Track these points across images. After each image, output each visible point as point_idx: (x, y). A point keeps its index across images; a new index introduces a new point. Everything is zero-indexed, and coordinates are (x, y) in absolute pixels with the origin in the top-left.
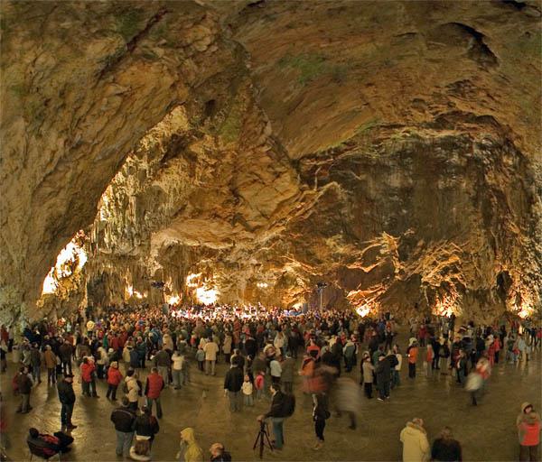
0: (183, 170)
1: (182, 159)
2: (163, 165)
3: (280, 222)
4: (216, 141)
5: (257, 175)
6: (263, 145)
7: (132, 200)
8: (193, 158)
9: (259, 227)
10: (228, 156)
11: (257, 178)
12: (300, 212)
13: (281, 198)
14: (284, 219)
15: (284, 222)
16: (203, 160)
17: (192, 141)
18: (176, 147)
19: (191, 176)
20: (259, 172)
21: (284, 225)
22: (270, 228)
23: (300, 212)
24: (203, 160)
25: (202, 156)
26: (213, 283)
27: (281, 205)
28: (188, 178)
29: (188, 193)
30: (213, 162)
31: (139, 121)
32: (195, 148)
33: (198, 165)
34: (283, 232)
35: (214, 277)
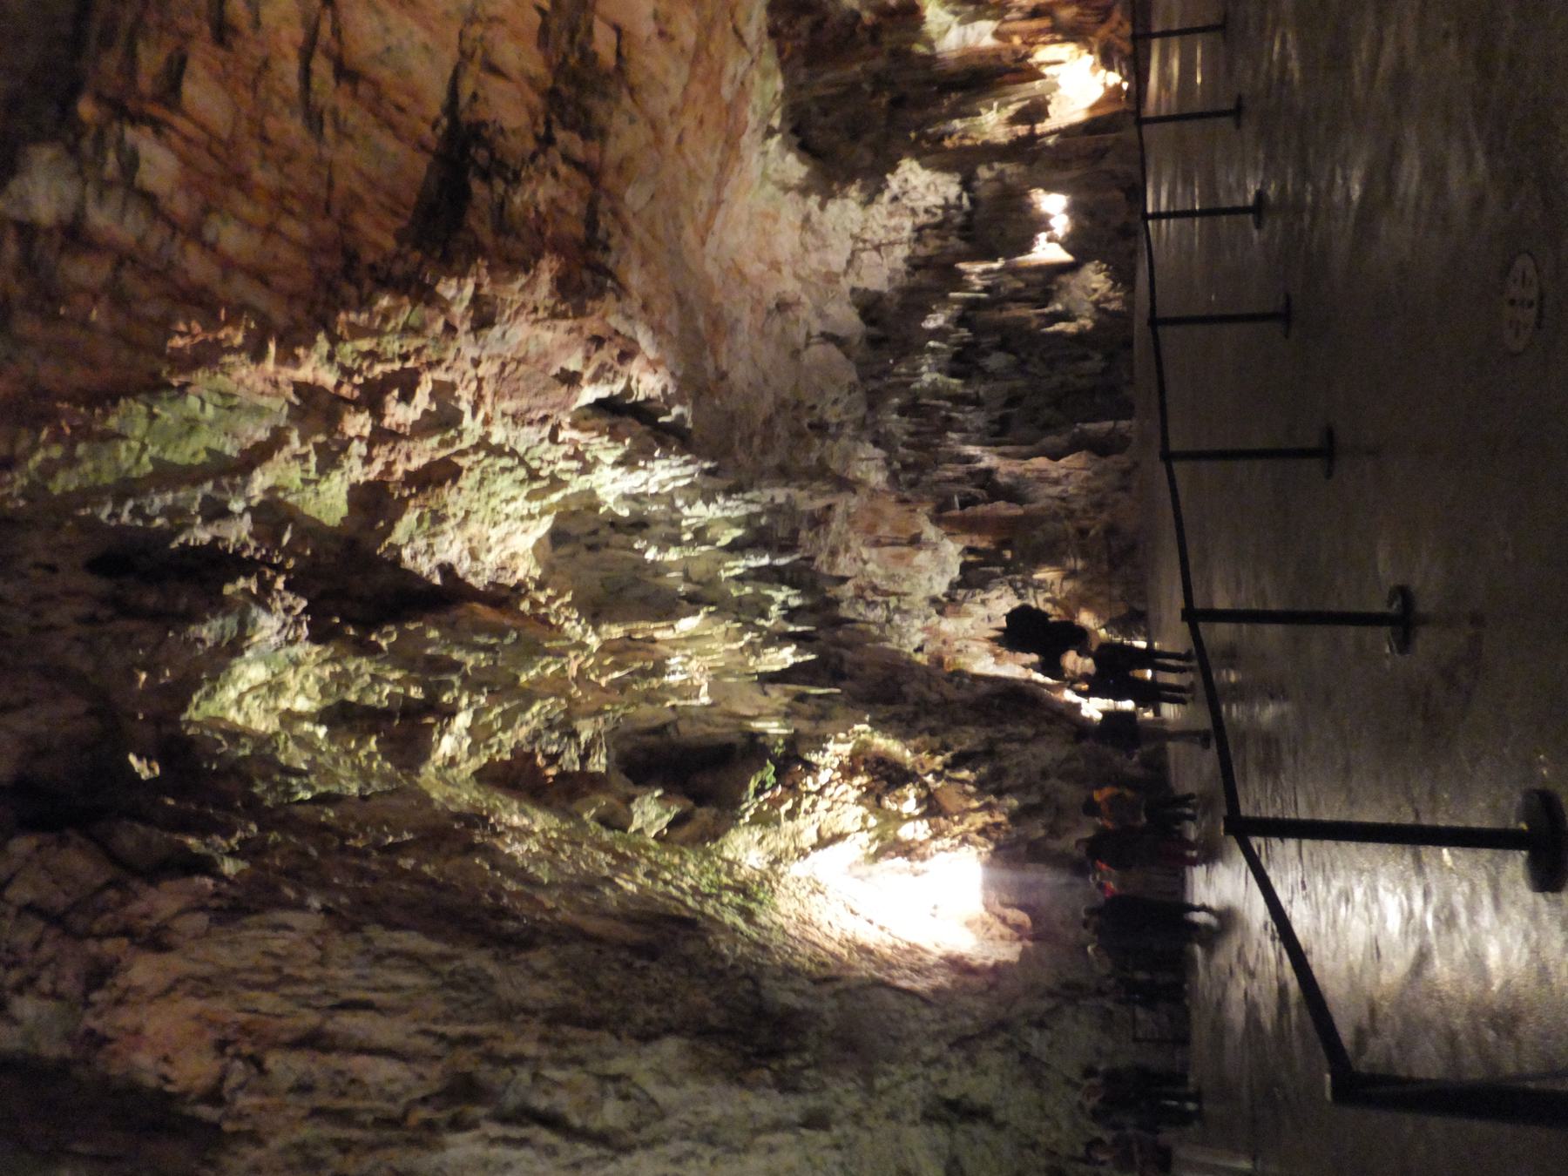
0: (438, 518)
1: (399, 534)
2: (450, 594)
4: (260, 454)
5: (306, 73)
6: (149, 199)
7: (616, 631)
8: (374, 503)
10: (305, 373)
11: (322, 67)
16: (368, 460)
17: (310, 530)
19: (455, 473)
20: (290, 68)
24: (368, 460)
25: (355, 471)
28: (467, 481)
29: (524, 439)
30: (357, 424)
31: (332, 971)
33: (399, 470)
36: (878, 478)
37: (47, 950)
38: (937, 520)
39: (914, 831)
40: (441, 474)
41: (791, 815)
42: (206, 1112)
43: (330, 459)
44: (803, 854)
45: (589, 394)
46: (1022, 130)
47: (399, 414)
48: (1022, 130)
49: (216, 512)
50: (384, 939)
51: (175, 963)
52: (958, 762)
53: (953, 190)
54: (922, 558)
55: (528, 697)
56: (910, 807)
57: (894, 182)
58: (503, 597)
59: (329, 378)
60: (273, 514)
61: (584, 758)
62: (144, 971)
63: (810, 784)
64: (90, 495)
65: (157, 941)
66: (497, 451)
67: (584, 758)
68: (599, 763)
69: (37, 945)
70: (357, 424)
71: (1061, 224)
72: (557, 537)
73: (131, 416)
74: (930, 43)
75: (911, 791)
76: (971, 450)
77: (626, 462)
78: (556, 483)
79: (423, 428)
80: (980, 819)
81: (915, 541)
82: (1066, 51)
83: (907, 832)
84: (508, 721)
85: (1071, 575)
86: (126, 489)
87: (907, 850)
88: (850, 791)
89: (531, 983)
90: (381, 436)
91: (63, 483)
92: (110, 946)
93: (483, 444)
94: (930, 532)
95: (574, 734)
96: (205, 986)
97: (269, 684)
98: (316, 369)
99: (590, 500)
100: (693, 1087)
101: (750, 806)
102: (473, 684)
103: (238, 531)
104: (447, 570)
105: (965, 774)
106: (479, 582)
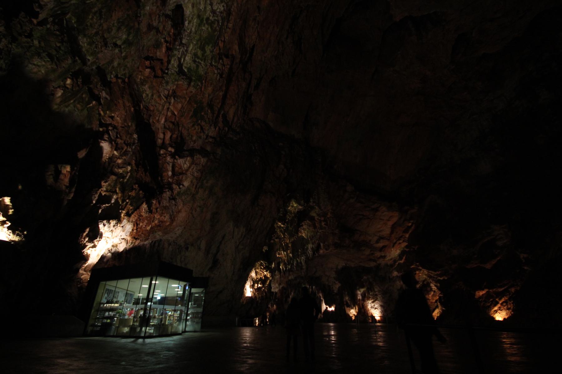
0: (309, 226)
1: (308, 221)
2: (299, 225)
3: (399, 239)
7: (290, 245)
8: (312, 219)
9: (384, 247)
10: (329, 214)
12: (413, 228)
13: (390, 223)
14: (401, 237)
15: (403, 239)
18: (301, 216)
21: (404, 241)
22: (393, 246)
23: (413, 228)
25: (316, 218)
26: (376, 295)
27: (393, 227)
30: (323, 219)
32: (313, 214)
34: (406, 247)
35: (376, 290)
36: (290, 278)
38: (283, 287)
40: (315, 227)
41: (261, 268)
43: (318, 215)
45: (322, 244)
46: (345, 303)
47: (323, 224)
48: (345, 303)
49: (314, 202)
52: (266, 293)
53: (335, 291)
54: (277, 285)
55: (284, 234)
56: (259, 285)
57: (337, 282)
58: (297, 232)
59: (328, 216)
66: (317, 233)
67: (273, 240)
68: (272, 241)
70: (323, 219)
71: (330, 309)
72: (303, 238)
74: (359, 289)
76: (292, 293)
77: (312, 248)
78: (311, 240)
80: (258, 296)
81: (280, 284)
82: (357, 310)
84: (281, 231)
85: (275, 311)
90: (321, 221)
93: (318, 232)
94: (281, 286)
97: (294, 206)
98: (329, 215)
99: (308, 243)
102: (287, 227)
103: (311, 204)
104: (302, 226)
105: (264, 294)
106: (300, 229)
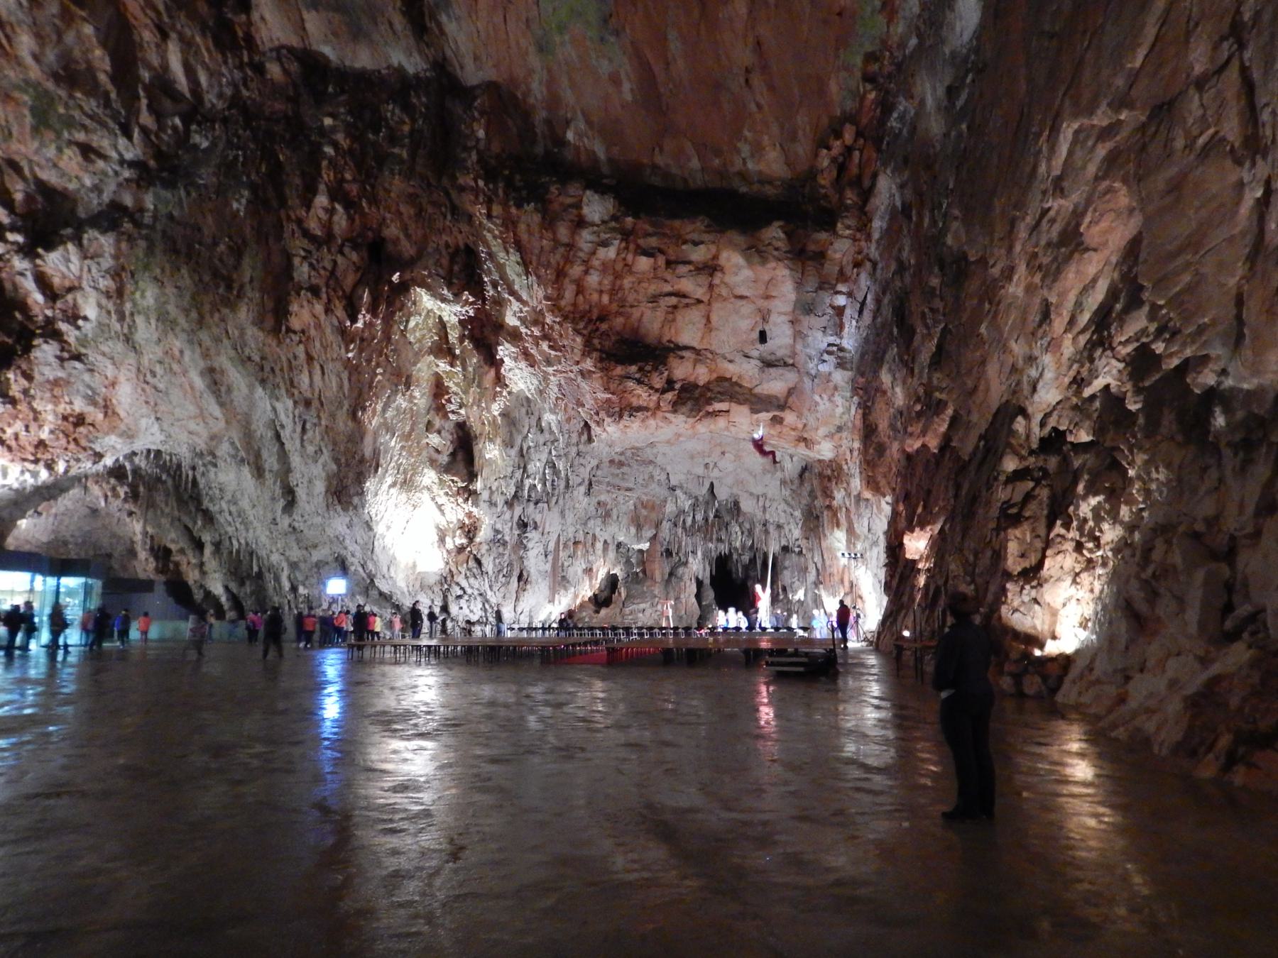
4: (519, 299)
8: (515, 336)
37: (322, 272)
39: (450, 544)
41: (447, 494)
42: (284, 328)
44: (433, 499)
47: (545, 346)
50: (345, 376)
51: (322, 317)
60: (499, 303)
61: (453, 412)
62: (319, 308)
63: (460, 500)
64: (488, 247)
65: (328, 311)
67: (453, 412)
69: (324, 268)
73: (515, 257)
75: (464, 541)
79: (542, 353)
83: (448, 540)
86: (491, 256)
87: (442, 540)
88: (461, 516)
89: (343, 424)
91: (489, 236)
92: (324, 296)
95: (461, 407)
96: (318, 326)
100: (324, 475)
101: (446, 477)
